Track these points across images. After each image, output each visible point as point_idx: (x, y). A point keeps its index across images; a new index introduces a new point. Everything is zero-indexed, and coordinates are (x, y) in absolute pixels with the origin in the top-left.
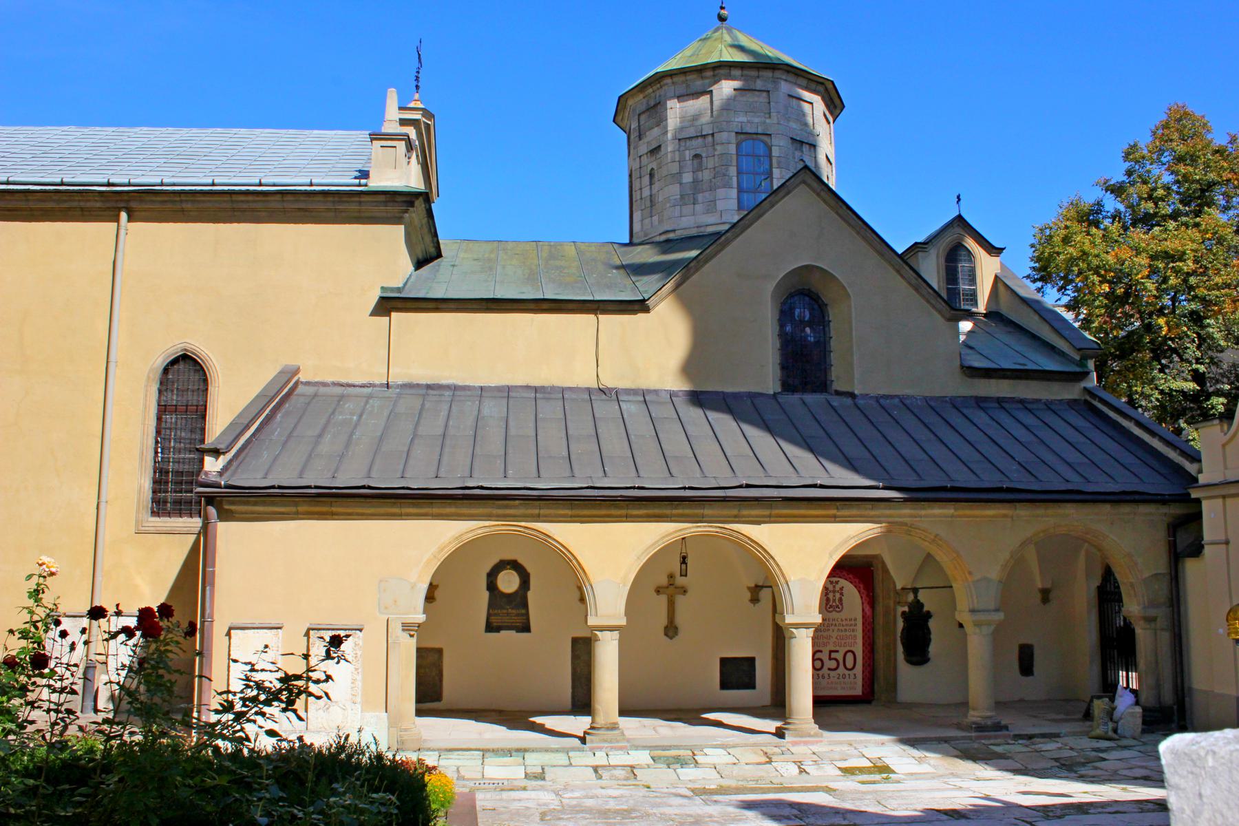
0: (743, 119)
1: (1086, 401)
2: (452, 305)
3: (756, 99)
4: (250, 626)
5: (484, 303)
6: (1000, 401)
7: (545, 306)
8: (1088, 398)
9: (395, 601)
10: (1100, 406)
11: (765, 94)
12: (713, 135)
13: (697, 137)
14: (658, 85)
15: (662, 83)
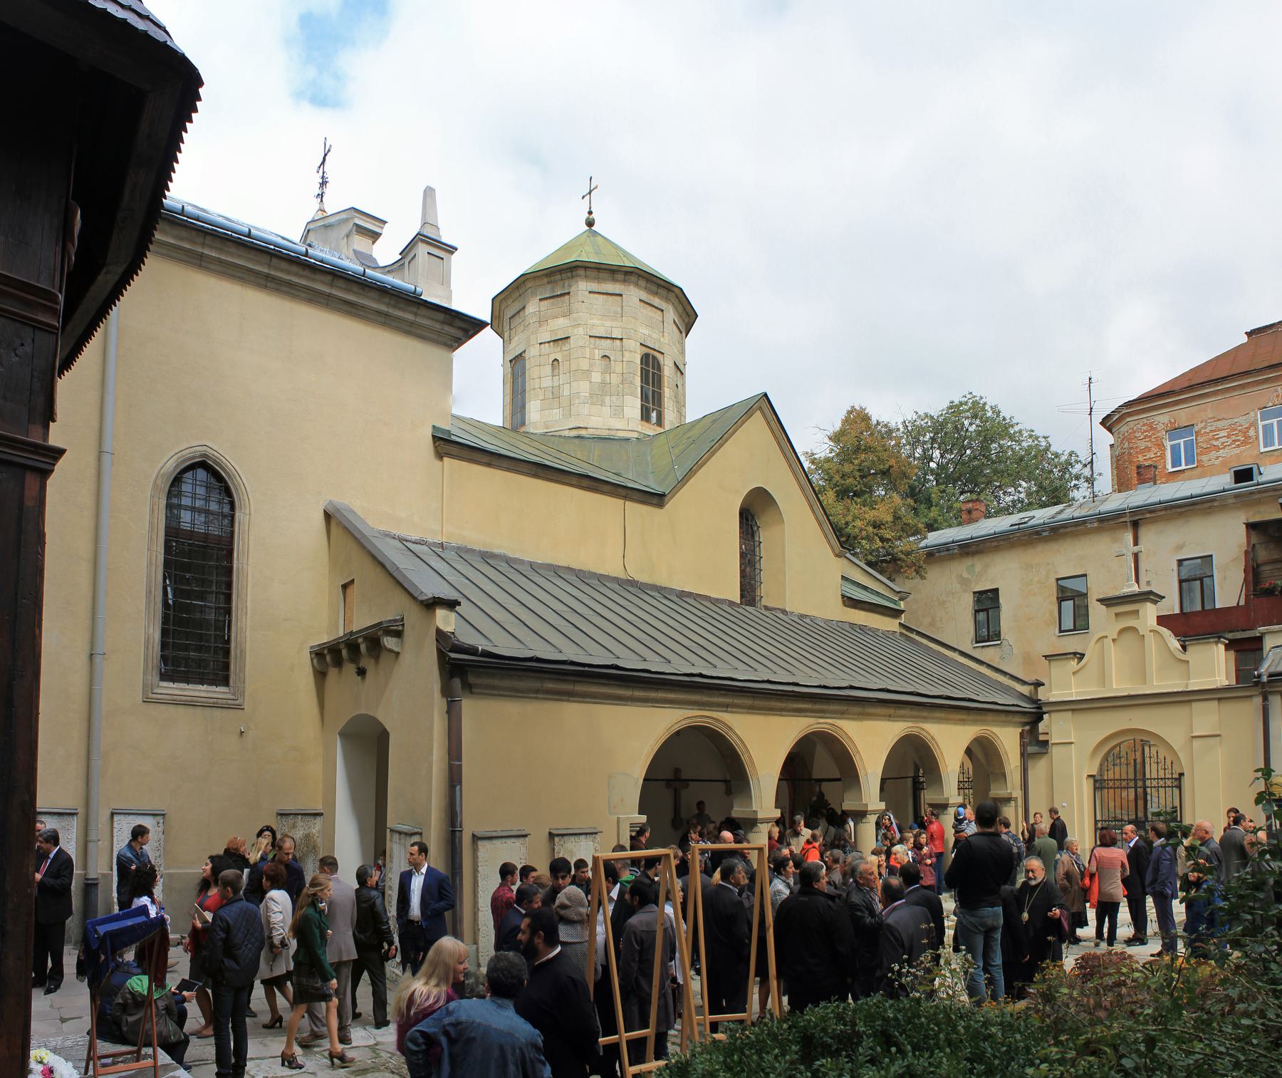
0: (646, 332)
1: (901, 634)
2: (505, 463)
3: (653, 315)
4: (494, 834)
5: (534, 468)
6: (862, 628)
7: (585, 483)
8: (904, 631)
9: (622, 800)
10: (918, 638)
11: (659, 312)
12: (621, 339)
13: (607, 338)
14: (569, 274)
15: (574, 273)
